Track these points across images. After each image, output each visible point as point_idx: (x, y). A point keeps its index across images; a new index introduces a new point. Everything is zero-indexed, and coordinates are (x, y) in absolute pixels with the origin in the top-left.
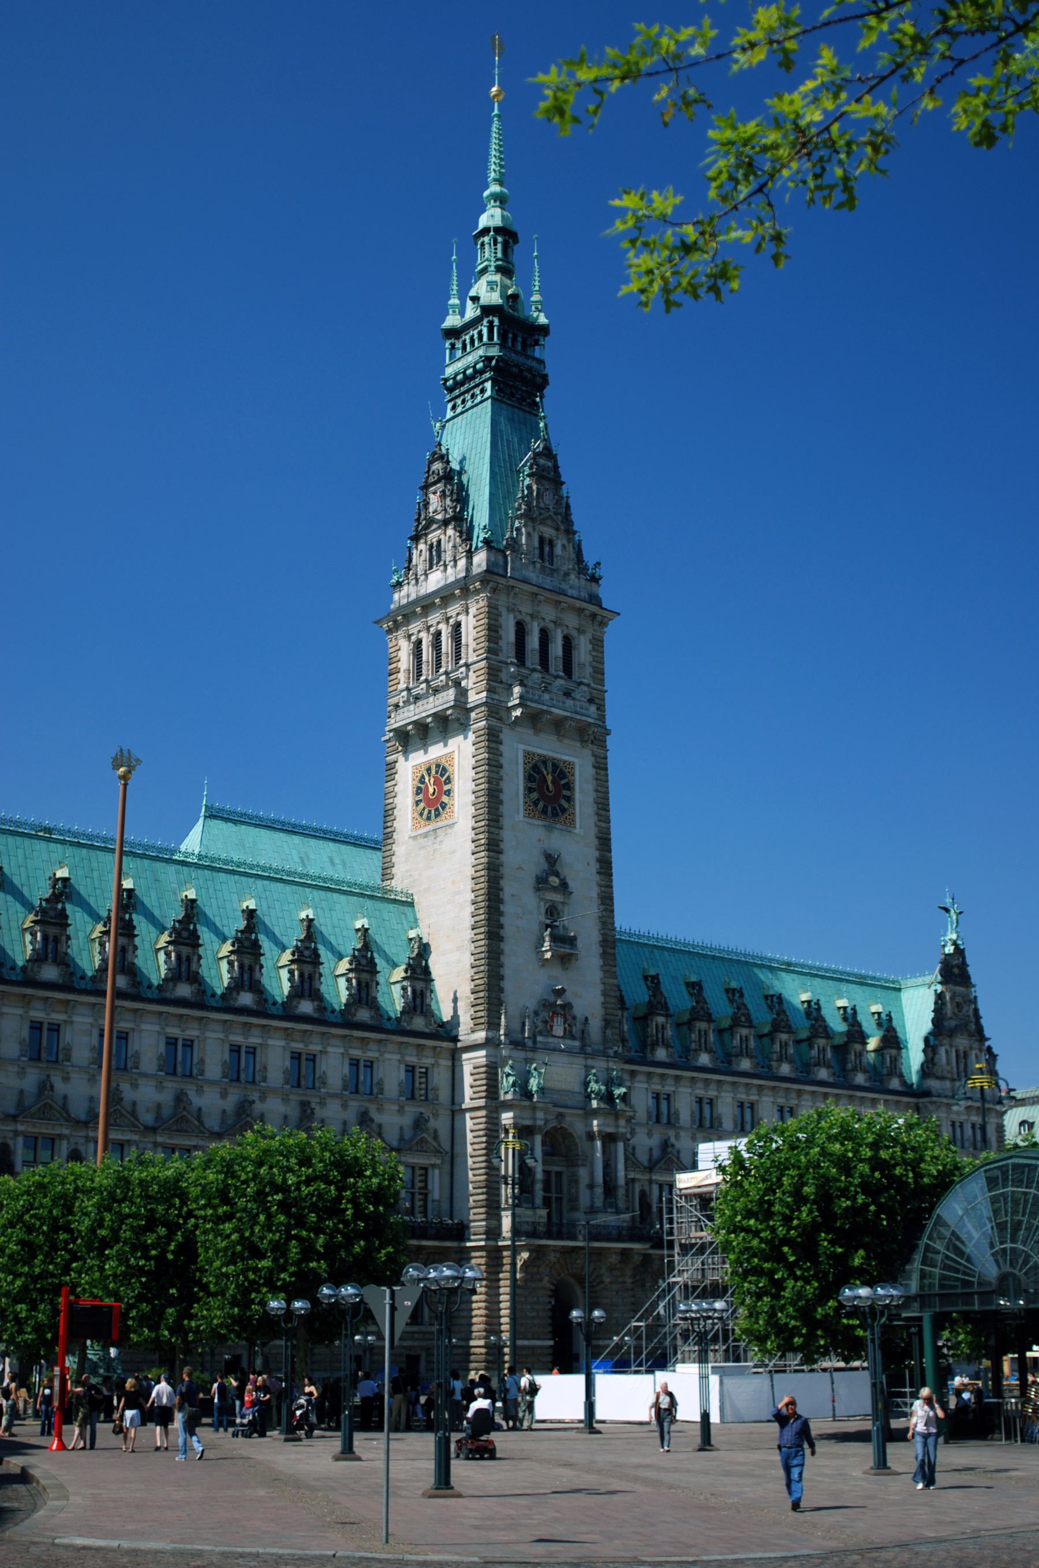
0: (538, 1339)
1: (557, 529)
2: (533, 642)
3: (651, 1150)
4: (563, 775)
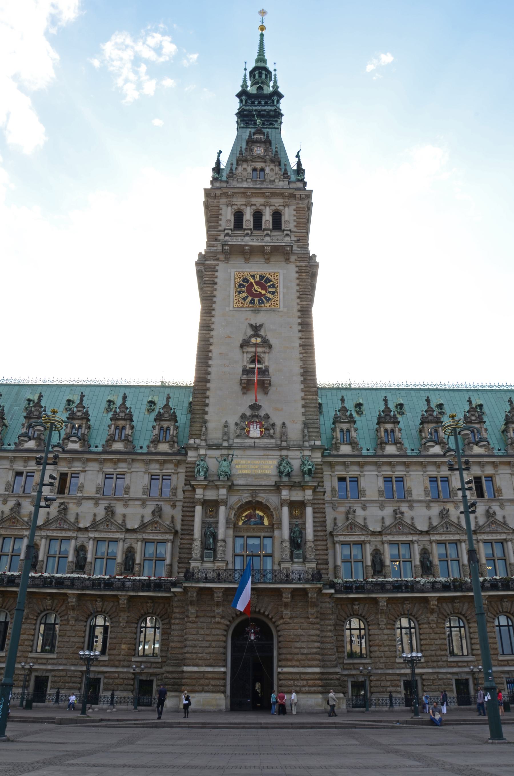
0: (210, 666)
1: (265, 162)
2: (248, 217)
3: (383, 518)
4: (268, 280)
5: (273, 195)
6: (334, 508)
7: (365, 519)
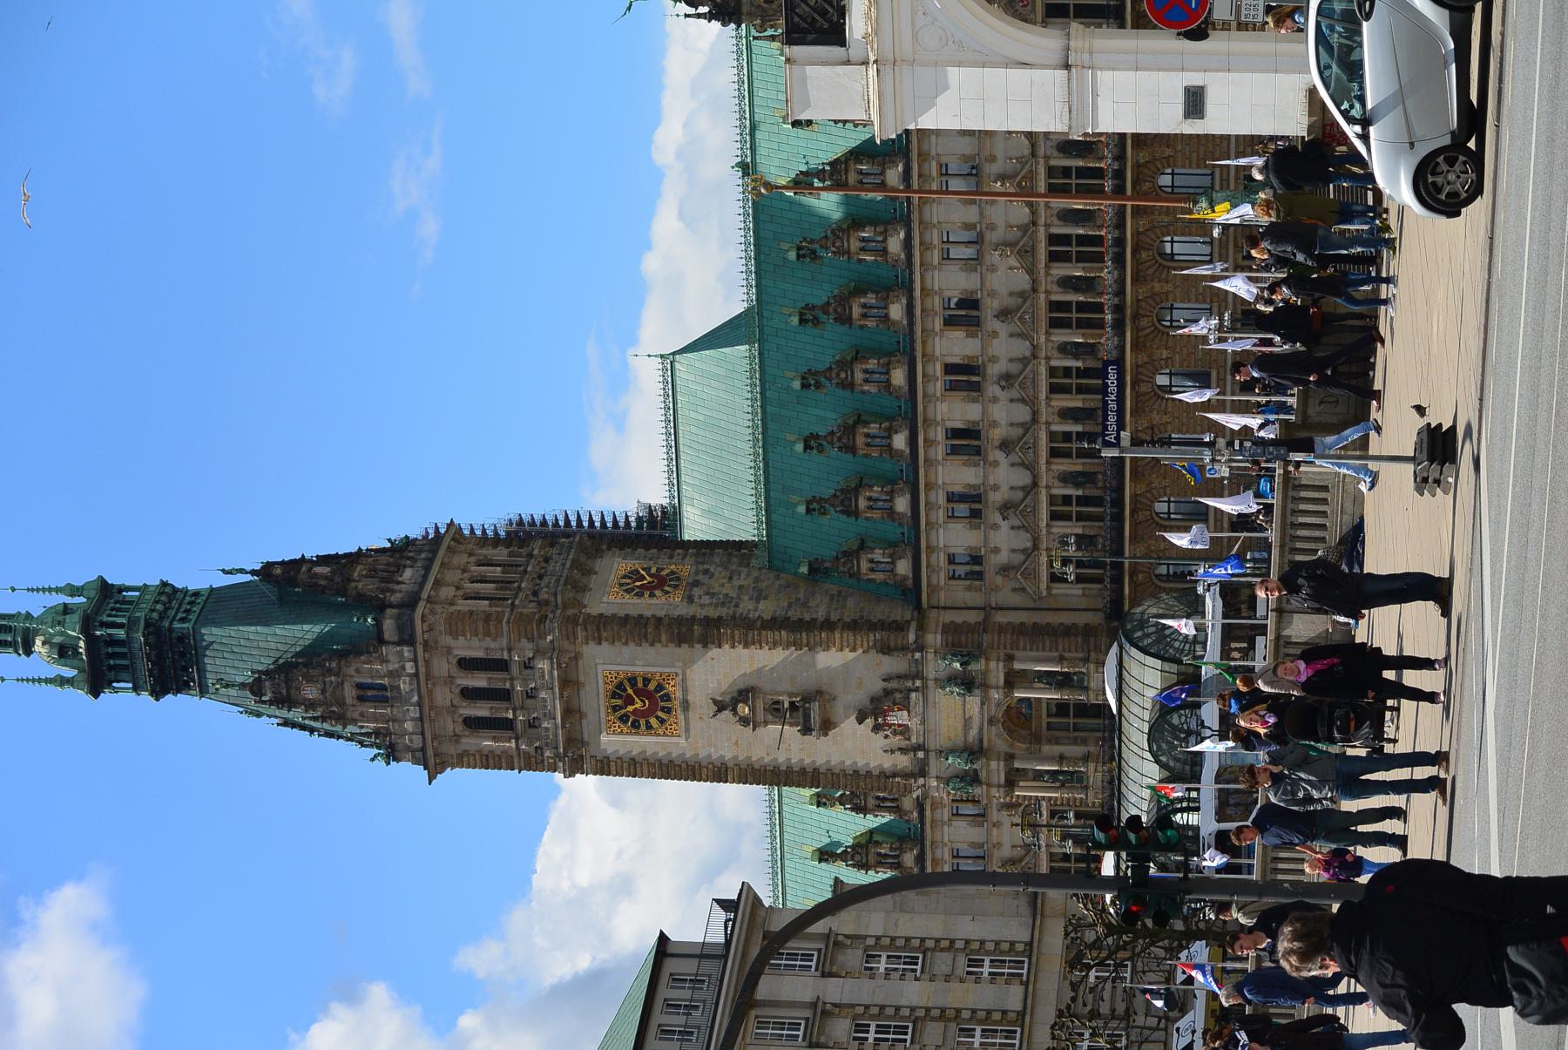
2: (482, 710)
4: (620, 686)
5: (428, 677)
6: (997, 589)
7: (1013, 551)
